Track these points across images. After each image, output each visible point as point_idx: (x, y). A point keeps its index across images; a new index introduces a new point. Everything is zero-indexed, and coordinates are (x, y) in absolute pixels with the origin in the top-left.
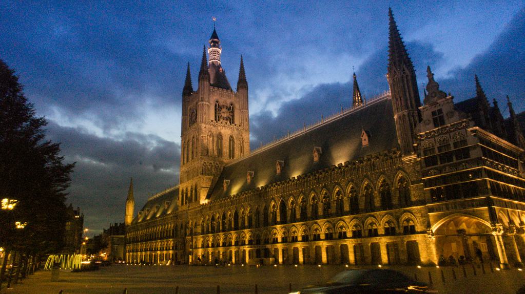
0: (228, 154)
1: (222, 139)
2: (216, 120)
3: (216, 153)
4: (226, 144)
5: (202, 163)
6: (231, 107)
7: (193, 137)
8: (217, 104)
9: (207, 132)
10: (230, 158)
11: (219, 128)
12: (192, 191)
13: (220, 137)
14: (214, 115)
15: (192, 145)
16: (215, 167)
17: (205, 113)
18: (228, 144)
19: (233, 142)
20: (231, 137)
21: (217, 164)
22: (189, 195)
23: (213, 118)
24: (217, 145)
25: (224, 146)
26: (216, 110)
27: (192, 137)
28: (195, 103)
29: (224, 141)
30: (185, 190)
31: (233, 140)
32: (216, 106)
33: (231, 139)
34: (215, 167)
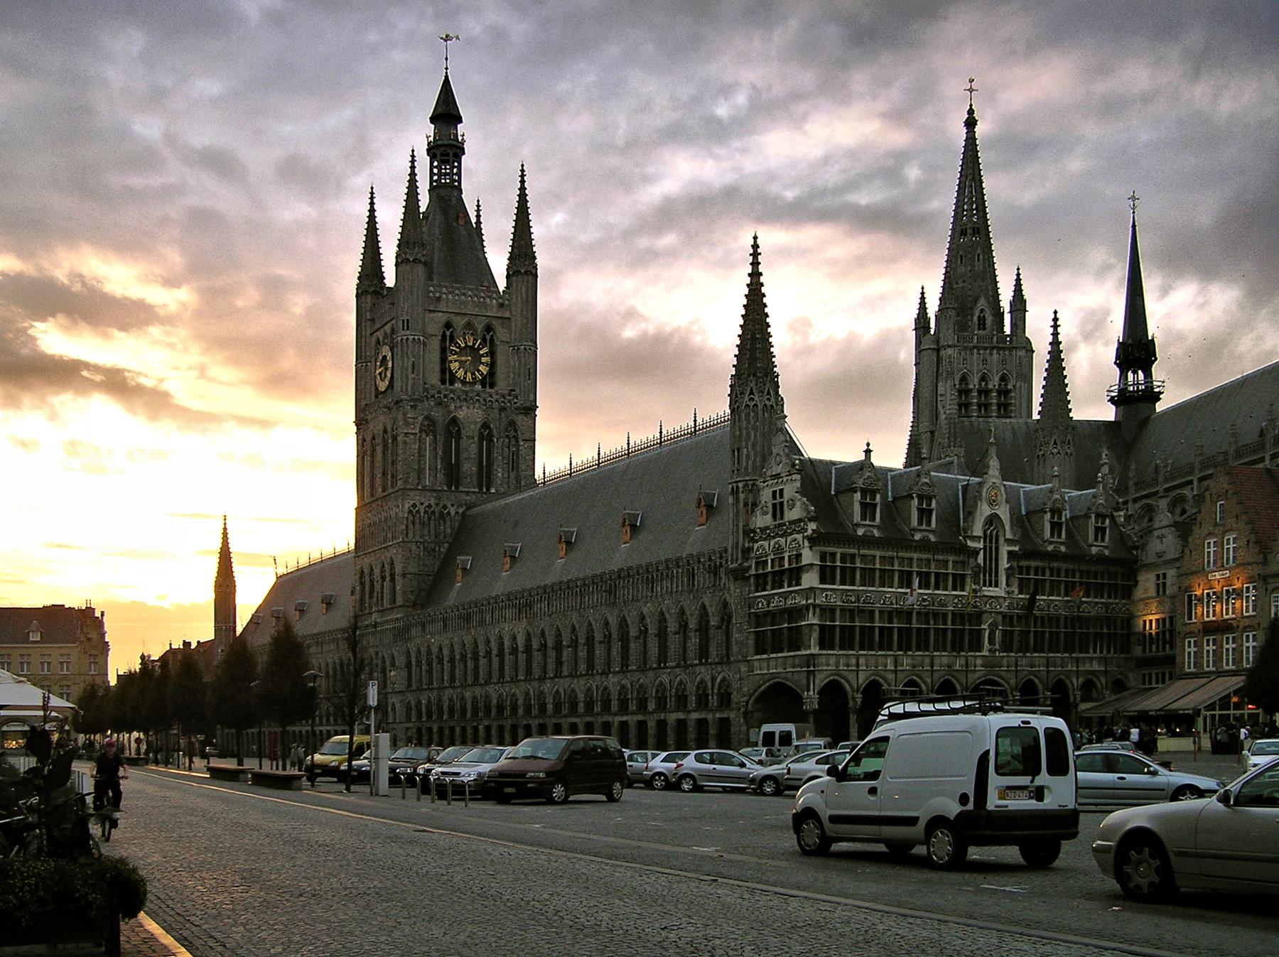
0: (474, 479)
1: (458, 436)
2: (443, 382)
3: (440, 477)
4: (470, 448)
5: (407, 506)
6: (488, 337)
7: (385, 431)
8: (448, 333)
9: (420, 419)
10: (481, 489)
11: (452, 407)
12: (383, 578)
13: (454, 427)
14: (437, 369)
15: (383, 452)
16: (441, 514)
17: (413, 366)
18: (476, 451)
19: (490, 439)
20: (485, 425)
21: (445, 507)
22: (377, 586)
23: (434, 379)
24: (447, 452)
25: (465, 455)
26: (444, 350)
27: (381, 427)
28: (388, 328)
29: (464, 442)
30: (366, 571)
31: (490, 435)
32: (444, 336)
33: (486, 433)
34: (441, 514)
